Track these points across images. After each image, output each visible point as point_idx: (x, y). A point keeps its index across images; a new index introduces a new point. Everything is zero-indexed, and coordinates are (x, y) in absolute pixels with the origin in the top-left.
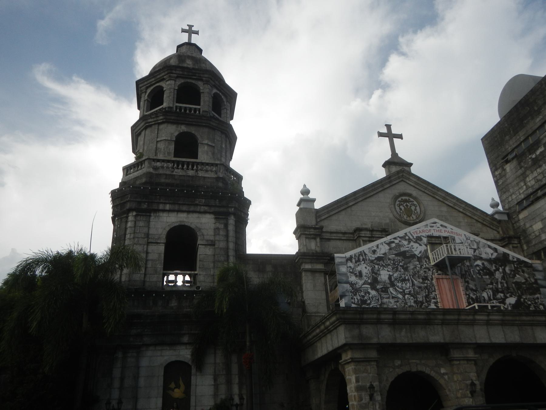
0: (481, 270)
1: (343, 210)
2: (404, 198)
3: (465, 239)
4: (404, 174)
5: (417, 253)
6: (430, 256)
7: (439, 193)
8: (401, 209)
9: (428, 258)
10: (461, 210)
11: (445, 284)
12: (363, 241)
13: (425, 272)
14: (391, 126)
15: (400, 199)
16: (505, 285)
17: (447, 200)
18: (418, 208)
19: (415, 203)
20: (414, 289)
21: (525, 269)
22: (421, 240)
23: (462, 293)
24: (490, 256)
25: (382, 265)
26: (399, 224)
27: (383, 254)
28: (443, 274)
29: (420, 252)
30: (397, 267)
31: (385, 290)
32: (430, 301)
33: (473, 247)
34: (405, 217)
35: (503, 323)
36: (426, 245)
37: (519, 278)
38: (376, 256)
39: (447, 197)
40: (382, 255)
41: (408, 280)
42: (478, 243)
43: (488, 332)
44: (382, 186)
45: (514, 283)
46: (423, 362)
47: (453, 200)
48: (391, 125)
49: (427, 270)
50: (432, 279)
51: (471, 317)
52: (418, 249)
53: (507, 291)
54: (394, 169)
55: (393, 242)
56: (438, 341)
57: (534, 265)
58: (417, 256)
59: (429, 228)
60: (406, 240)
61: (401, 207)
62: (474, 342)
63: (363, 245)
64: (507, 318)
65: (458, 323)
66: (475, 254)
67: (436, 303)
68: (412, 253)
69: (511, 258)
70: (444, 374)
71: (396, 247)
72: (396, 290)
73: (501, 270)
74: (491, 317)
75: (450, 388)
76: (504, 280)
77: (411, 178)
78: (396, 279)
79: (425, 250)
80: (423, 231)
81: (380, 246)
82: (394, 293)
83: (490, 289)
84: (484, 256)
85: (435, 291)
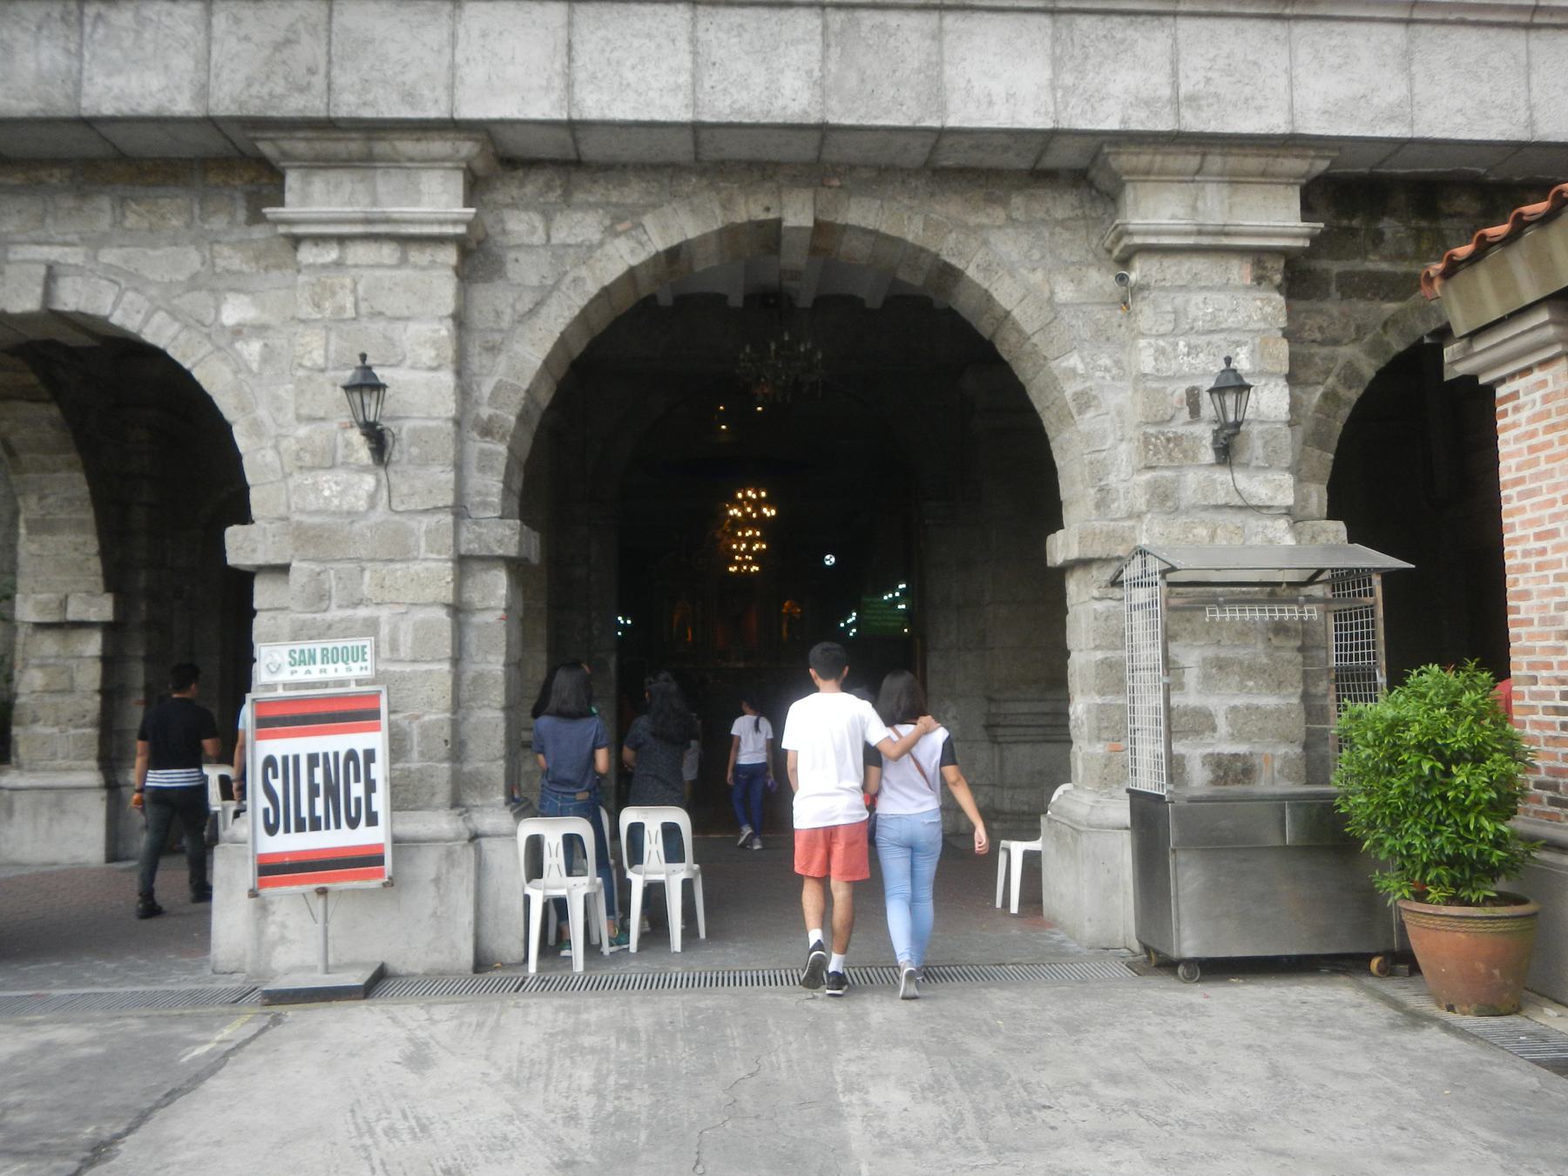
43: (570, 46)
46: (109, 256)
56: (147, 108)
62: (433, 112)
70: (238, 332)
75: (262, 413)
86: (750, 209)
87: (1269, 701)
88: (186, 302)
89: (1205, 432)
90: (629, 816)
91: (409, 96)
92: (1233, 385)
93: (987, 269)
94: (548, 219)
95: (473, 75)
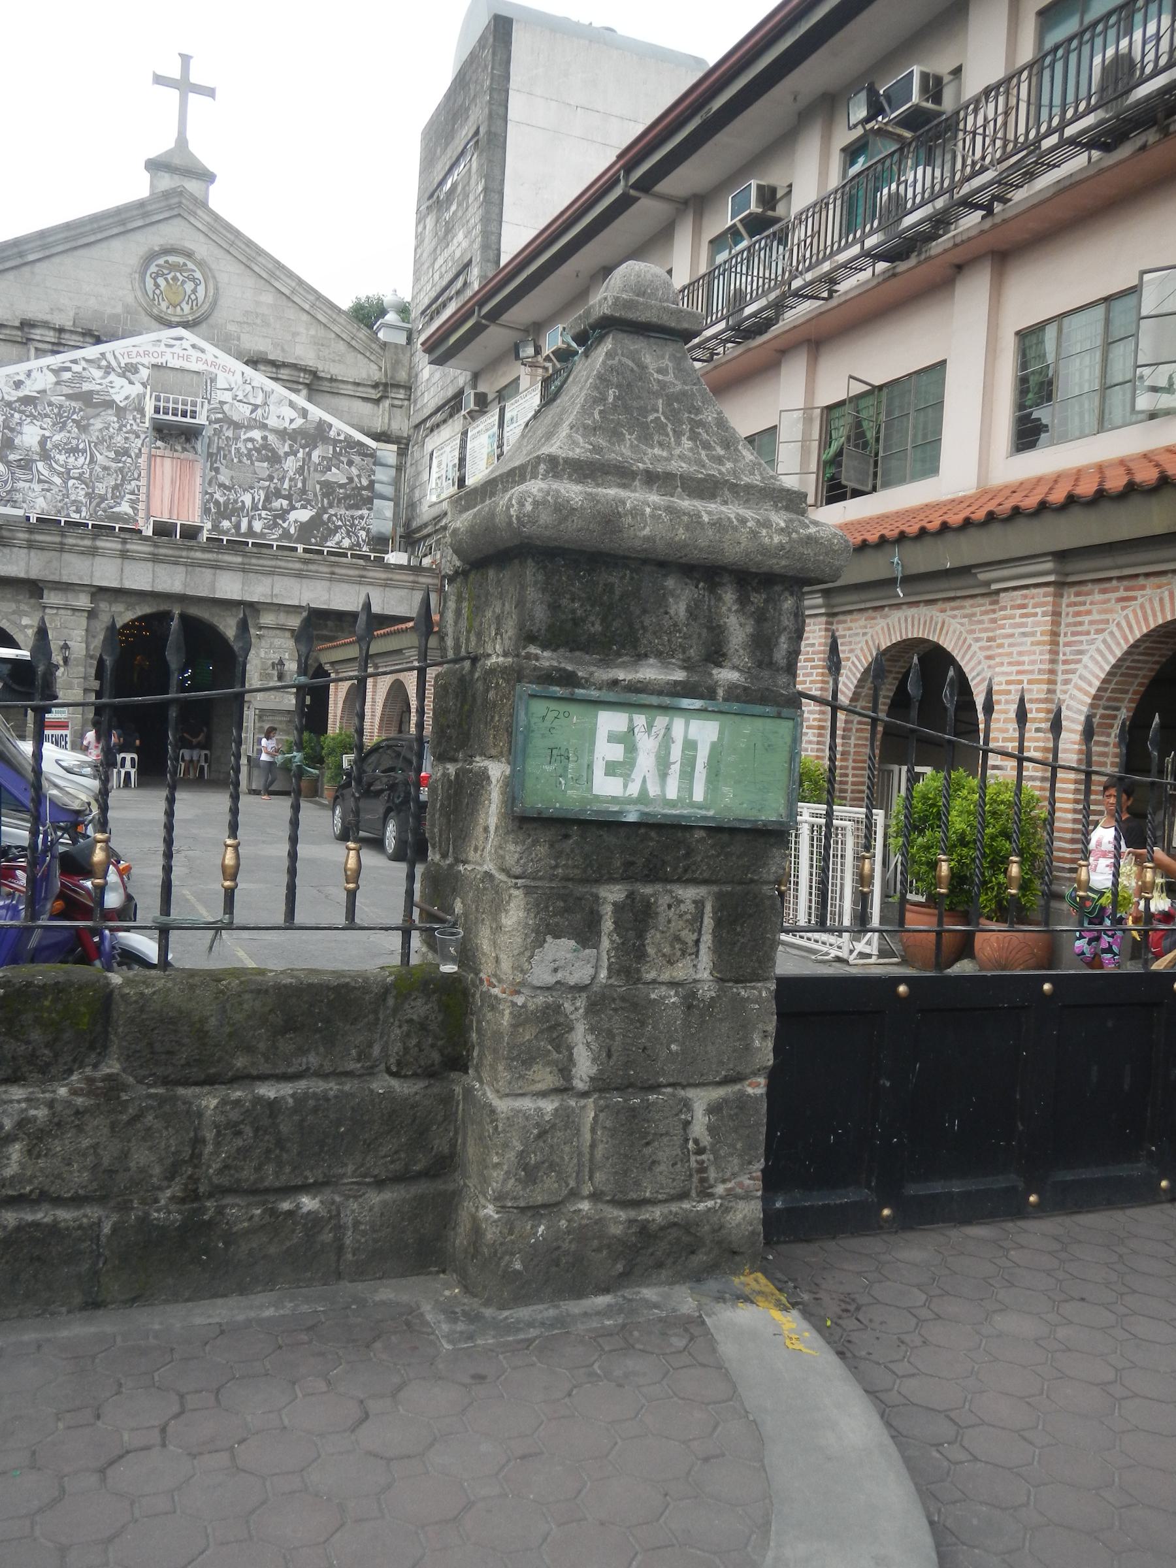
0: (255, 449)
1: (12, 268)
2: (172, 259)
3: (240, 381)
4: (184, 201)
5: (118, 398)
6: (147, 409)
7: (260, 259)
8: (157, 286)
9: (141, 411)
10: (307, 307)
11: (166, 468)
12: (36, 349)
13: (126, 438)
14: (192, 61)
15: (161, 261)
16: (300, 485)
17: (277, 278)
18: (201, 290)
19: (198, 275)
20: (91, 471)
21: (357, 459)
22: (136, 371)
23: (198, 489)
24: (287, 424)
25: (32, 415)
26: (146, 319)
27: (38, 392)
28: (165, 448)
29: (127, 398)
30: (64, 424)
31: (26, 464)
32: (122, 498)
33: (252, 401)
34: (164, 305)
35: (155, 559)
36: (144, 385)
37: (336, 475)
38: (21, 394)
39: (278, 273)
40: (35, 394)
41: (84, 451)
42: (267, 395)
44: (123, 223)
45: (318, 482)
47: (289, 281)
48: (191, 57)
49: (132, 436)
50: (139, 455)
51: (87, 542)
52: (122, 390)
53: (300, 497)
54: (167, 182)
55: (68, 369)
56: (13, 575)
57: (379, 453)
58: (117, 405)
59: (163, 348)
60: (99, 367)
61: (161, 281)
63: (36, 358)
64: (162, 551)
65: (61, 548)
66: (253, 416)
67: (133, 504)
68: (107, 398)
69: (332, 434)
70: (26, 626)
71: (71, 381)
72: (51, 466)
73: (300, 455)
74: (129, 547)
76: (301, 474)
77: (199, 212)
78: (56, 446)
79: (138, 395)
80: (146, 353)
81: (34, 374)
82: (46, 473)
83: (263, 488)
84: (272, 422)
85: (138, 479)
86: (164, 607)
87: (284, 738)
88: (13, 617)
89: (275, 673)
90: (123, 755)
91: (81, 579)
92: (281, 663)
93: (225, 627)
94: (110, 605)
95: (97, 574)
